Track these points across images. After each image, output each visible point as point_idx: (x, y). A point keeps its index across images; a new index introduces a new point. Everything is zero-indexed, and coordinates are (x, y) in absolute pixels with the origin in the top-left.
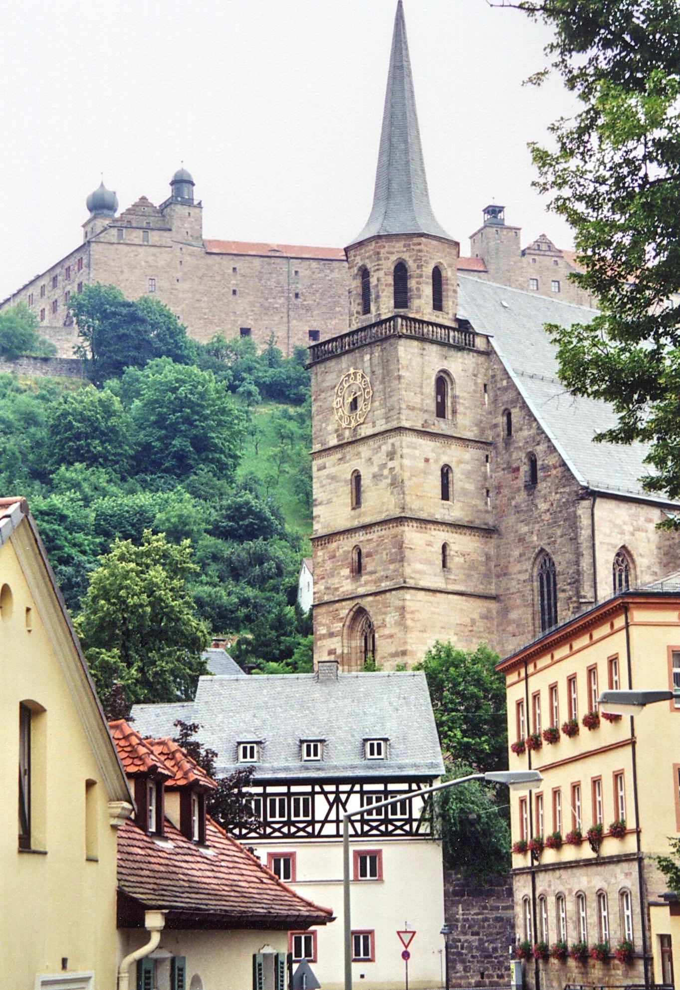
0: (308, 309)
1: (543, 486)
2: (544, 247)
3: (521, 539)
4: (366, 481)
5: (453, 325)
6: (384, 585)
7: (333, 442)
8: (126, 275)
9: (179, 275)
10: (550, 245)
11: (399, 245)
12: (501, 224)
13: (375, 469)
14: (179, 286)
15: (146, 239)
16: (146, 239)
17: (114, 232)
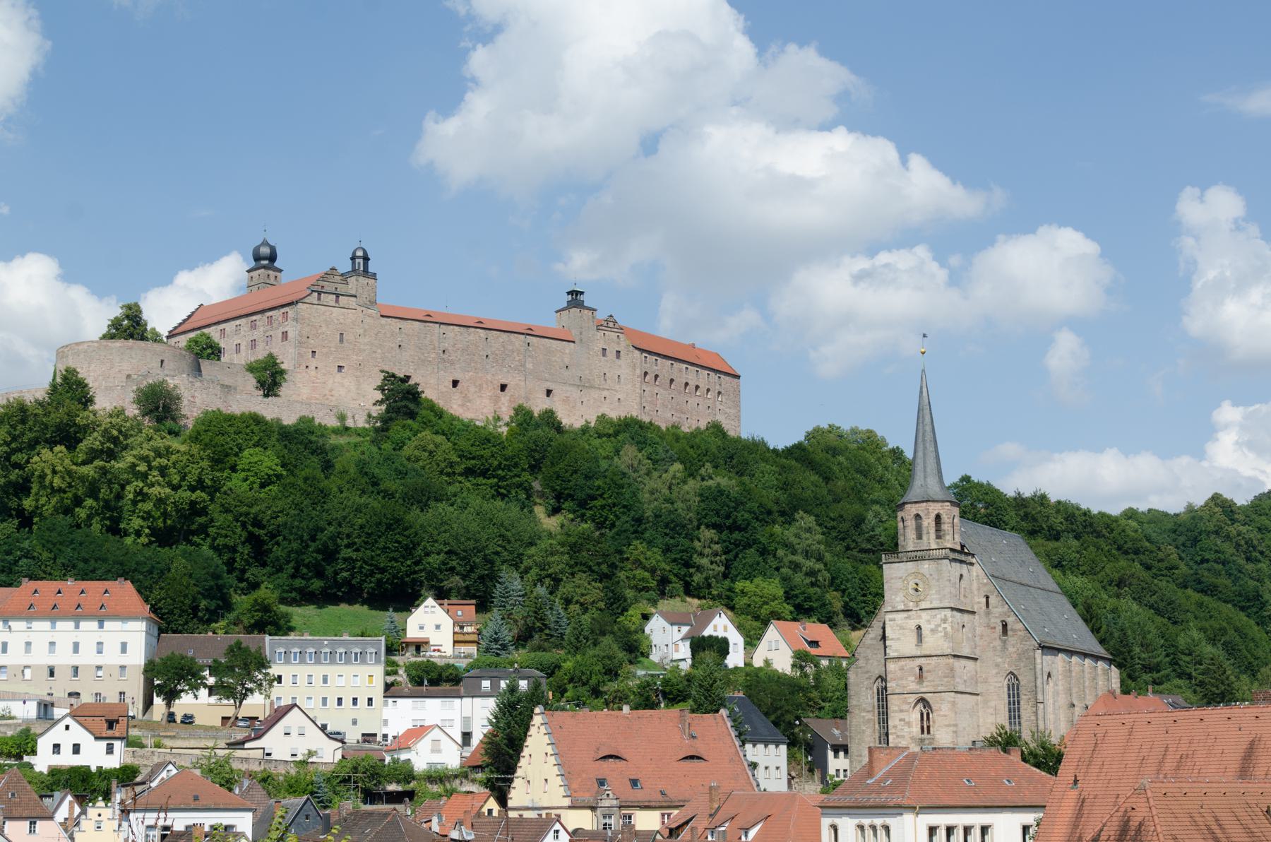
0: (452, 363)
1: (1012, 640)
2: (611, 325)
3: (997, 665)
4: (925, 632)
5: (959, 548)
6: (940, 689)
7: (901, 607)
8: (324, 329)
9: (361, 331)
10: (615, 322)
11: (939, 505)
12: (580, 305)
13: (933, 626)
14: (361, 340)
15: (337, 301)
16: (337, 301)
17: (315, 294)
